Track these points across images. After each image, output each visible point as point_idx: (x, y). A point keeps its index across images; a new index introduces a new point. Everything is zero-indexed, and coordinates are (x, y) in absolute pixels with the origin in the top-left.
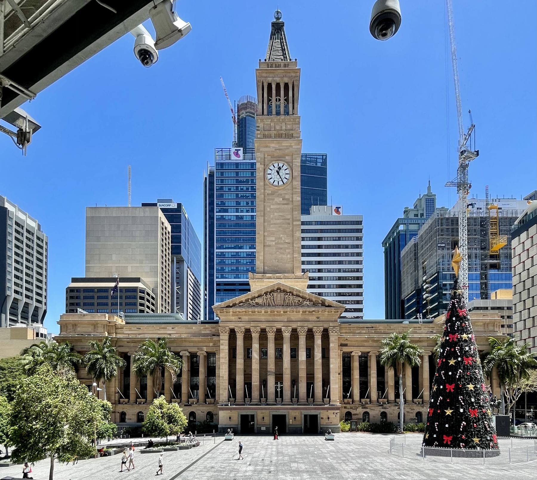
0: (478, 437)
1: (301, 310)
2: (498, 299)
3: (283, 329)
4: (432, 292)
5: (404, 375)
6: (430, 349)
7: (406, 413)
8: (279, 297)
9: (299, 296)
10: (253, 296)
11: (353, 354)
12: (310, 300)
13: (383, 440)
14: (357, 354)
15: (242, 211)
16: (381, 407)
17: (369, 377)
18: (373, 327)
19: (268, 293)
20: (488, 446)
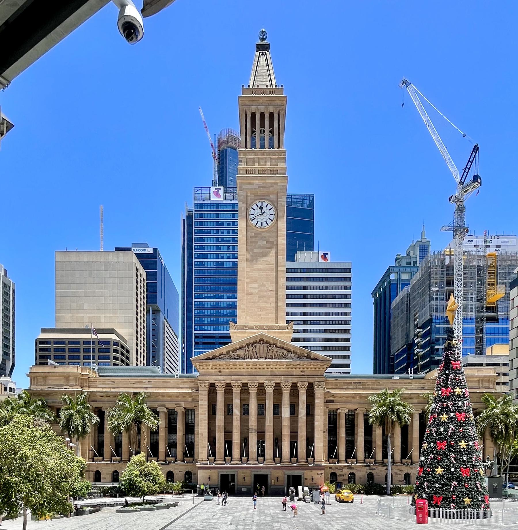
0: (469, 498)
1: (285, 362)
2: (493, 354)
3: (266, 383)
4: (424, 347)
5: (393, 434)
6: (421, 406)
7: (394, 475)
8: (261, 349)
9: (283, 348)
10: (234, 347)
11: (339, 411)
12: (295, 353)
13: (369, 502)
14: (343, 412)
15: (222, 257)
16: (368, 468)
17: (355, 436)
18: (360, 383)
19: (251, 345)
20: (479, 507)
